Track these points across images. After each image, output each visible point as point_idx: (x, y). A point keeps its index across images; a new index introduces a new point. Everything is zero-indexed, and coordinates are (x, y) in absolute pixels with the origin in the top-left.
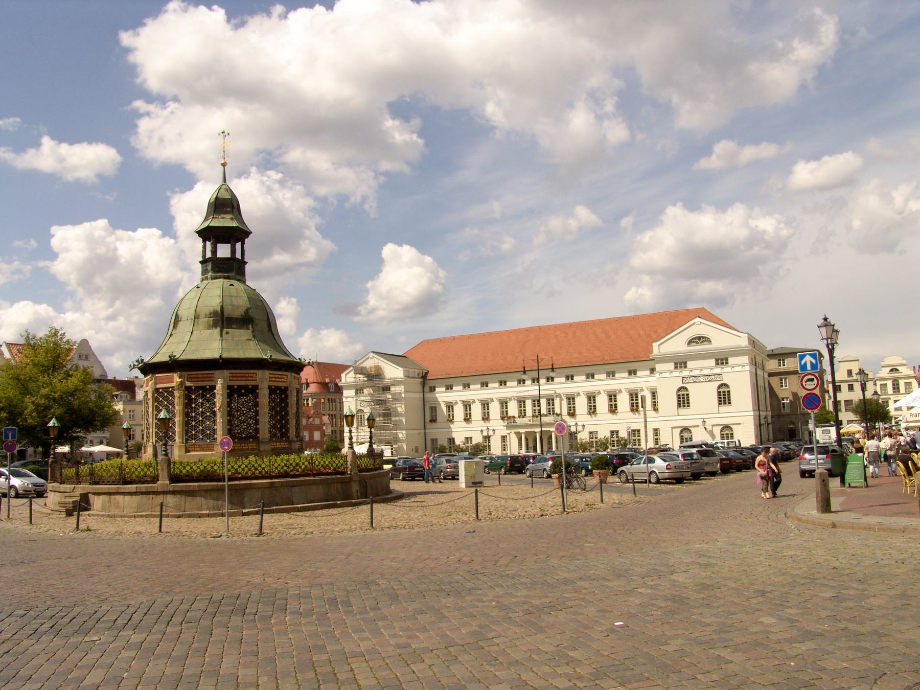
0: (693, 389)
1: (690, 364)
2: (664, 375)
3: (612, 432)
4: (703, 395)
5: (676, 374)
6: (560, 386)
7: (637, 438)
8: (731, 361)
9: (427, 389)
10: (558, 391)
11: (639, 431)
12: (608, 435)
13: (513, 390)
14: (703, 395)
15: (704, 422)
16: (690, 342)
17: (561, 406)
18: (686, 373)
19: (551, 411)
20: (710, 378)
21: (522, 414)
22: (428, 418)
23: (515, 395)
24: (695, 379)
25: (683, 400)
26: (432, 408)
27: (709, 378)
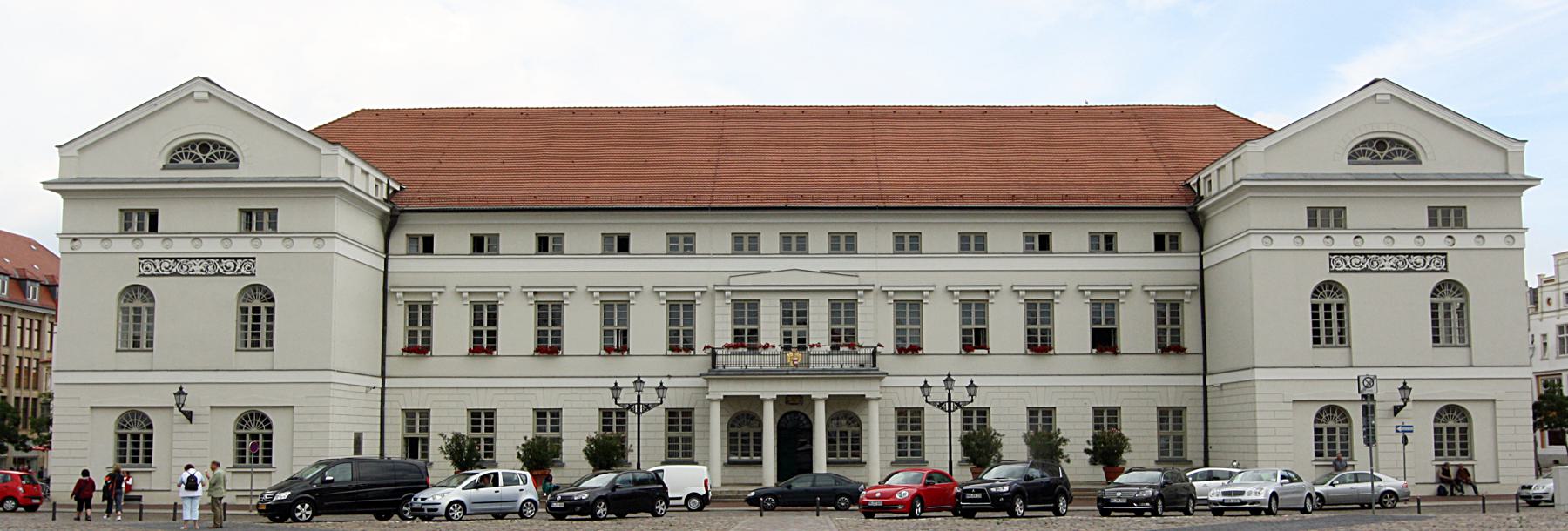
4: (1389, 312)
5: (1315, 240)
6: (876, 265)
9: (399, 242)
10: (865, 279)
11: (1179, 412)
13: (713, 265)
14: (1389, 312)
15: (1404, 387)
16: (1353, 157)
17: (876, 326)
19: (843, 339)
21: (746, 339)
22: (398, 339)
23: (721, 279)
24: (1368, 262)
25: (1329, 319)
26: (412, 307)
27: (1407, 262)
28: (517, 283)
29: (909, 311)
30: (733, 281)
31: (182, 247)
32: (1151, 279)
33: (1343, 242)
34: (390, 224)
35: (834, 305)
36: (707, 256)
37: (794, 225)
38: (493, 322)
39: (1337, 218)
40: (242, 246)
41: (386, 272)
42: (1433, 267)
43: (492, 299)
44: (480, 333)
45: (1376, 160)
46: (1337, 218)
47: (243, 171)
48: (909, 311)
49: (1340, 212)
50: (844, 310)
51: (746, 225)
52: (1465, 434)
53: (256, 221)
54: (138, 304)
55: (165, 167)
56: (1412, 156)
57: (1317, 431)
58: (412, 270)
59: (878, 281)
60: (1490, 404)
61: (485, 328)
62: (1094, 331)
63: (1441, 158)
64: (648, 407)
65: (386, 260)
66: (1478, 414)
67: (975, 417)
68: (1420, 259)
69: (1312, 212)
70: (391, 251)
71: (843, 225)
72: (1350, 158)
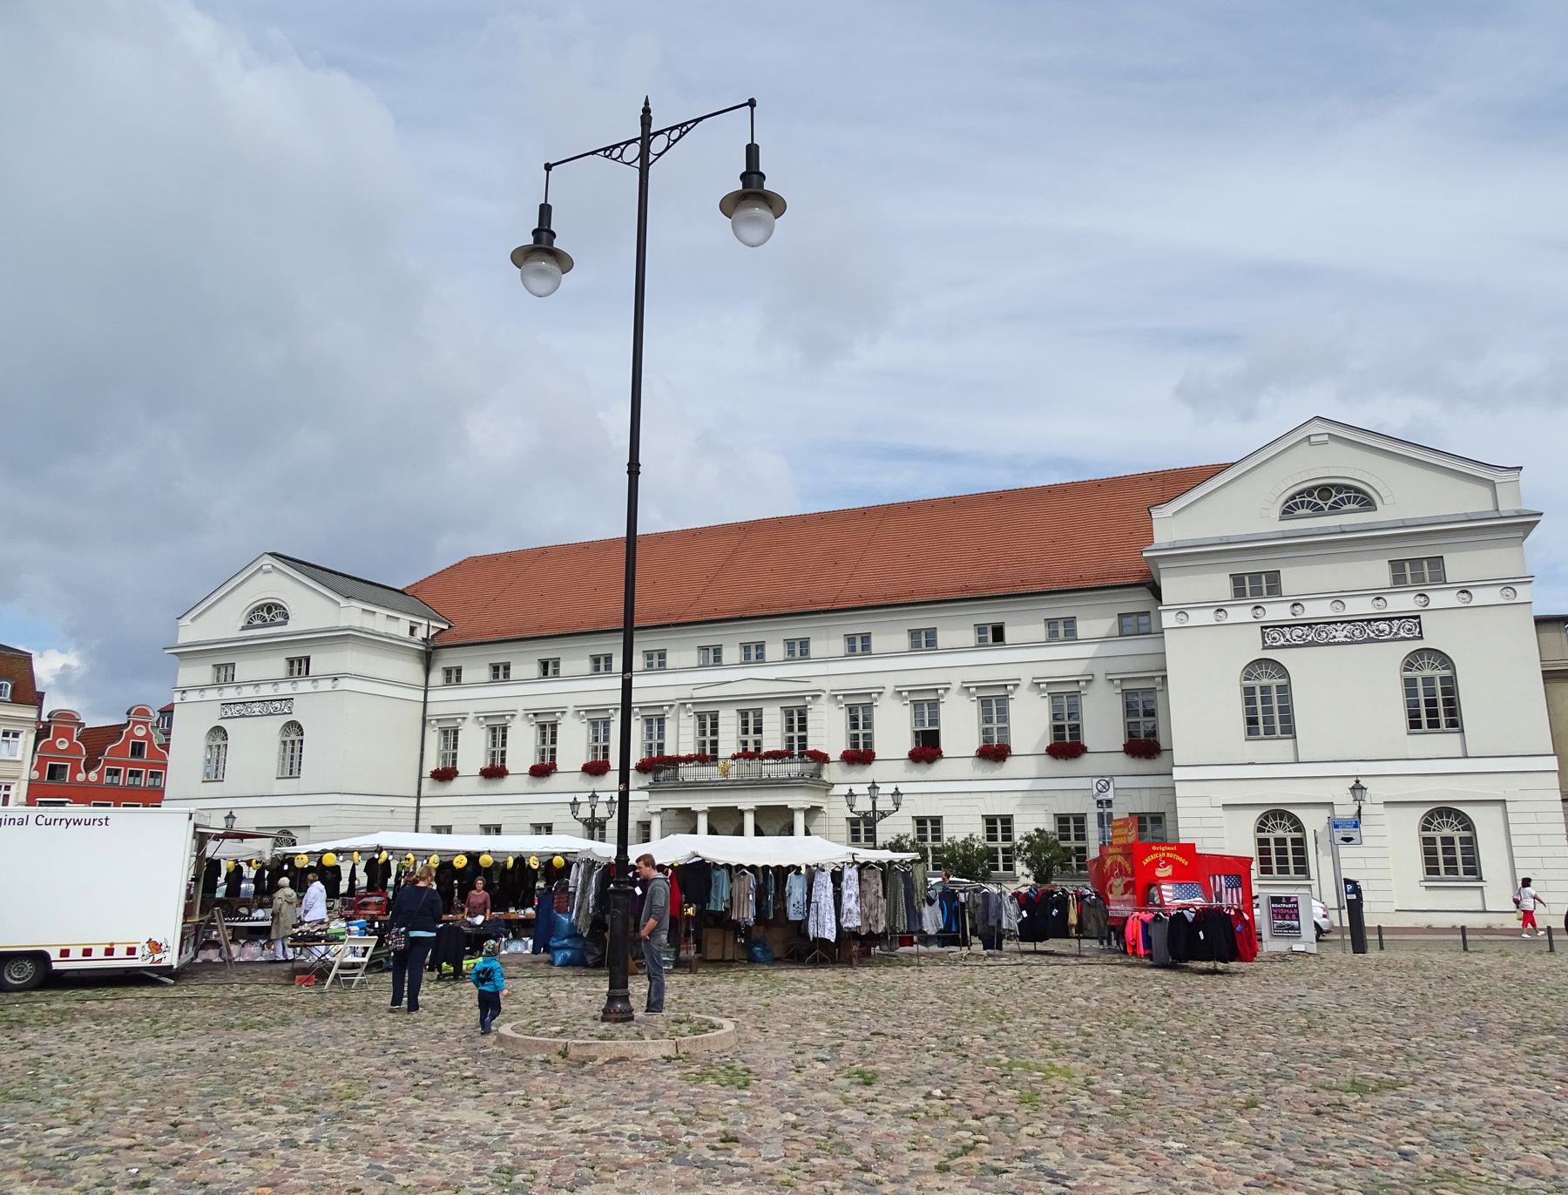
0: (1307, 670)
1: (1294, 578)
2: (1196, 617)
3: (990, 821)
5: (1241, 613)
7: (1072, 844)
8: (1458, 565)
9: (437, 677)
12: (979, 831)
16: (1288, 511)
18: (1277, 612)
20: (1370, 631)
22: (432, 763)
24: (1314, 633)
27: (1366, 630)
28: (889, 683)
29: (859, 715)
30: (697, 694)
31: (248, 693)
32: (1113, 666)
33: (1277, 612)
34: (427, 657)
35: (789, 713)
36: (675, 671)
37: (752, 633)
38: (803, 728)
39: (1272, 585)
40: (285, 689)
41: (425, 702)
42: (1402, 634)
43: (800, 703)
44: (651, 746)
45: (1318, 510)
46: (1272, 585)
47: (291, 627)
48: (859, 715)
49: (1274, 577)
50: (797, 719)
51: (710, 637)
52: (1470, 844)
53: (299, 667)
54: (293, 737)
55: (243, 628)
56: (1366, 502)
57: (1426, 841)
58: (445, 700)
59: (828, 685)
60: (1498, 809)
61: (796, 734)
62: (917, 734)
63: (1405, 498)
64: (884, 815)
65: (426, 692)
66: (1486, 824)
67: (1072, 824)
68: (1383, 626)
69: (1237, 579)
70: (431, 682)
71: (796, 630)
72: (1284, 512)
